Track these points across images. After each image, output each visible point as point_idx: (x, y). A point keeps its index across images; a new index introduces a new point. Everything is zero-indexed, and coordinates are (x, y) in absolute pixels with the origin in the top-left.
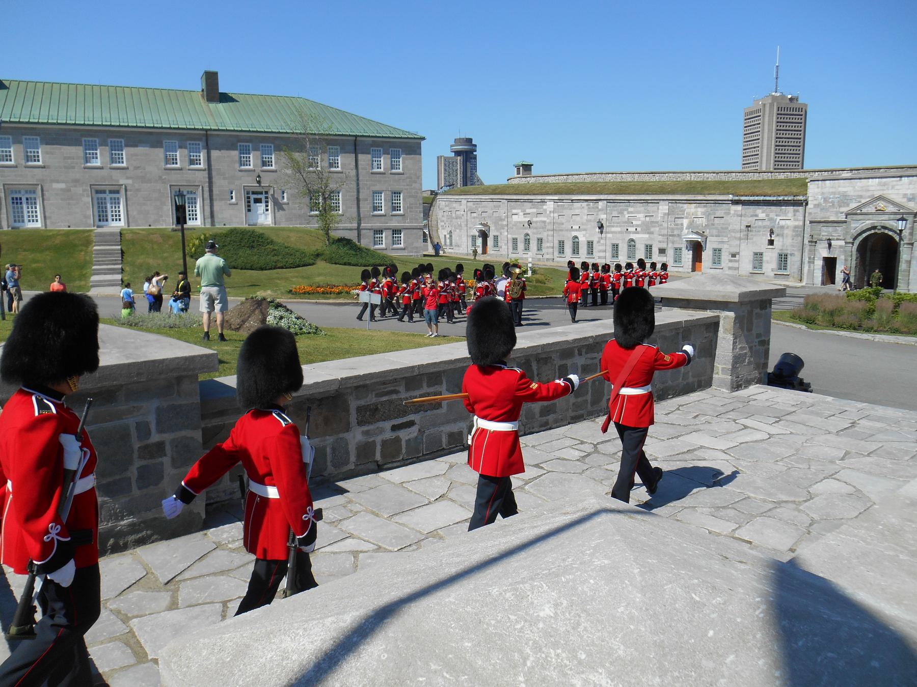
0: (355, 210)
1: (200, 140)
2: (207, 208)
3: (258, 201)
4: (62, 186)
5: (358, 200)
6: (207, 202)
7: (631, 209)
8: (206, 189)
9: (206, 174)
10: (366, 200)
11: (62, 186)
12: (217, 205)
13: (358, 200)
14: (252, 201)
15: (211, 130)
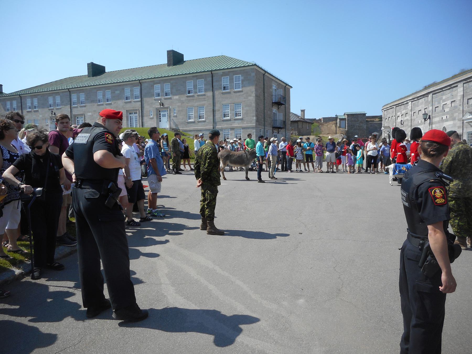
0: (212, 118)
1: (138, 86)
2: (141, 120)
3: (164, 116)
4: (90, 114)
5: (214, 111)
6: (141, 118)
7: (444, 97)
8: (140, 111)
9: (140, 103)
10: (219, 110)
11: (90, 114)
12: (145, 119)
13: (214, 111)
14: (161, 116)
15: (141, 80)
